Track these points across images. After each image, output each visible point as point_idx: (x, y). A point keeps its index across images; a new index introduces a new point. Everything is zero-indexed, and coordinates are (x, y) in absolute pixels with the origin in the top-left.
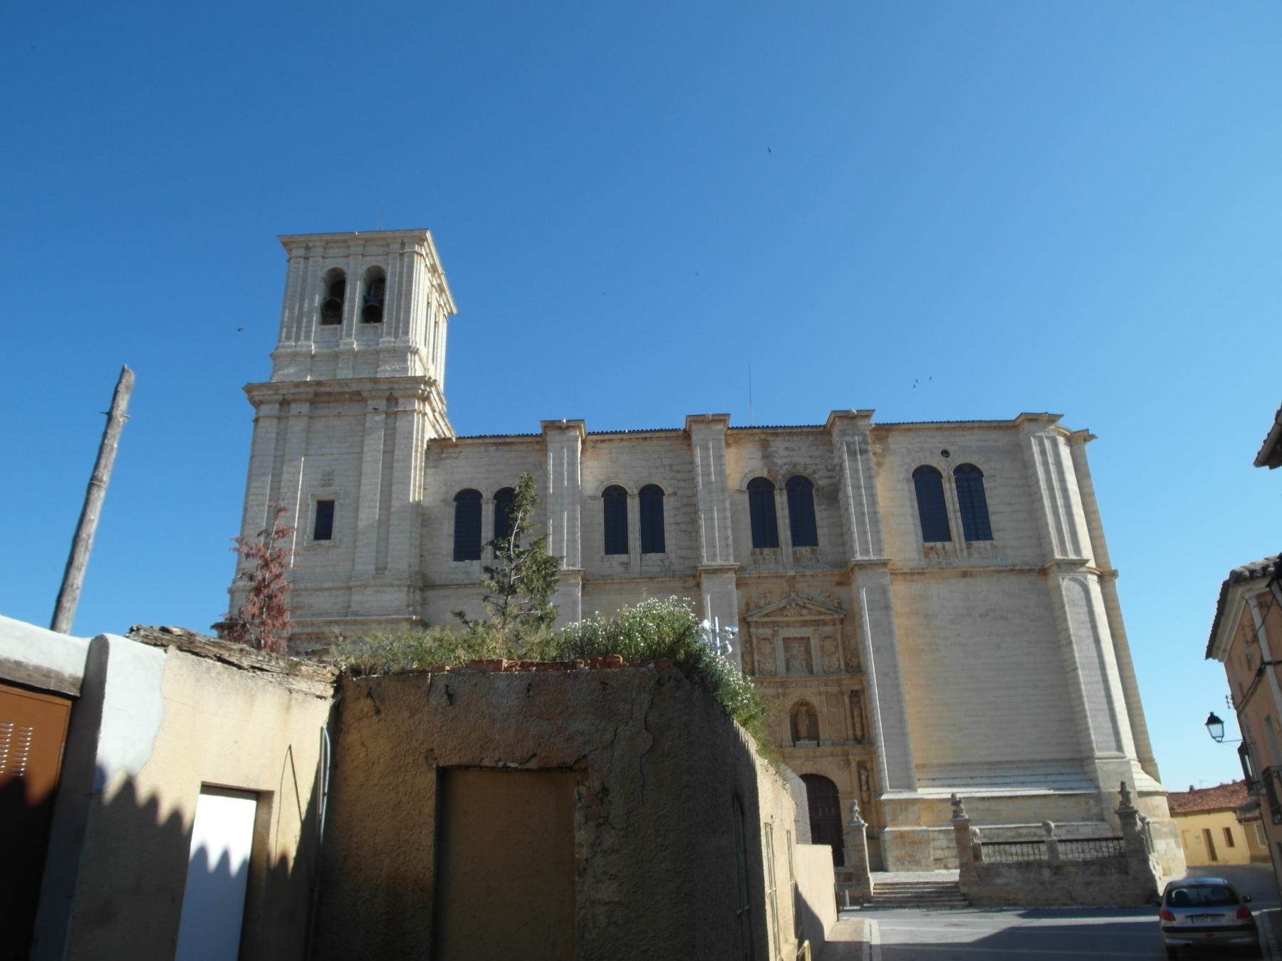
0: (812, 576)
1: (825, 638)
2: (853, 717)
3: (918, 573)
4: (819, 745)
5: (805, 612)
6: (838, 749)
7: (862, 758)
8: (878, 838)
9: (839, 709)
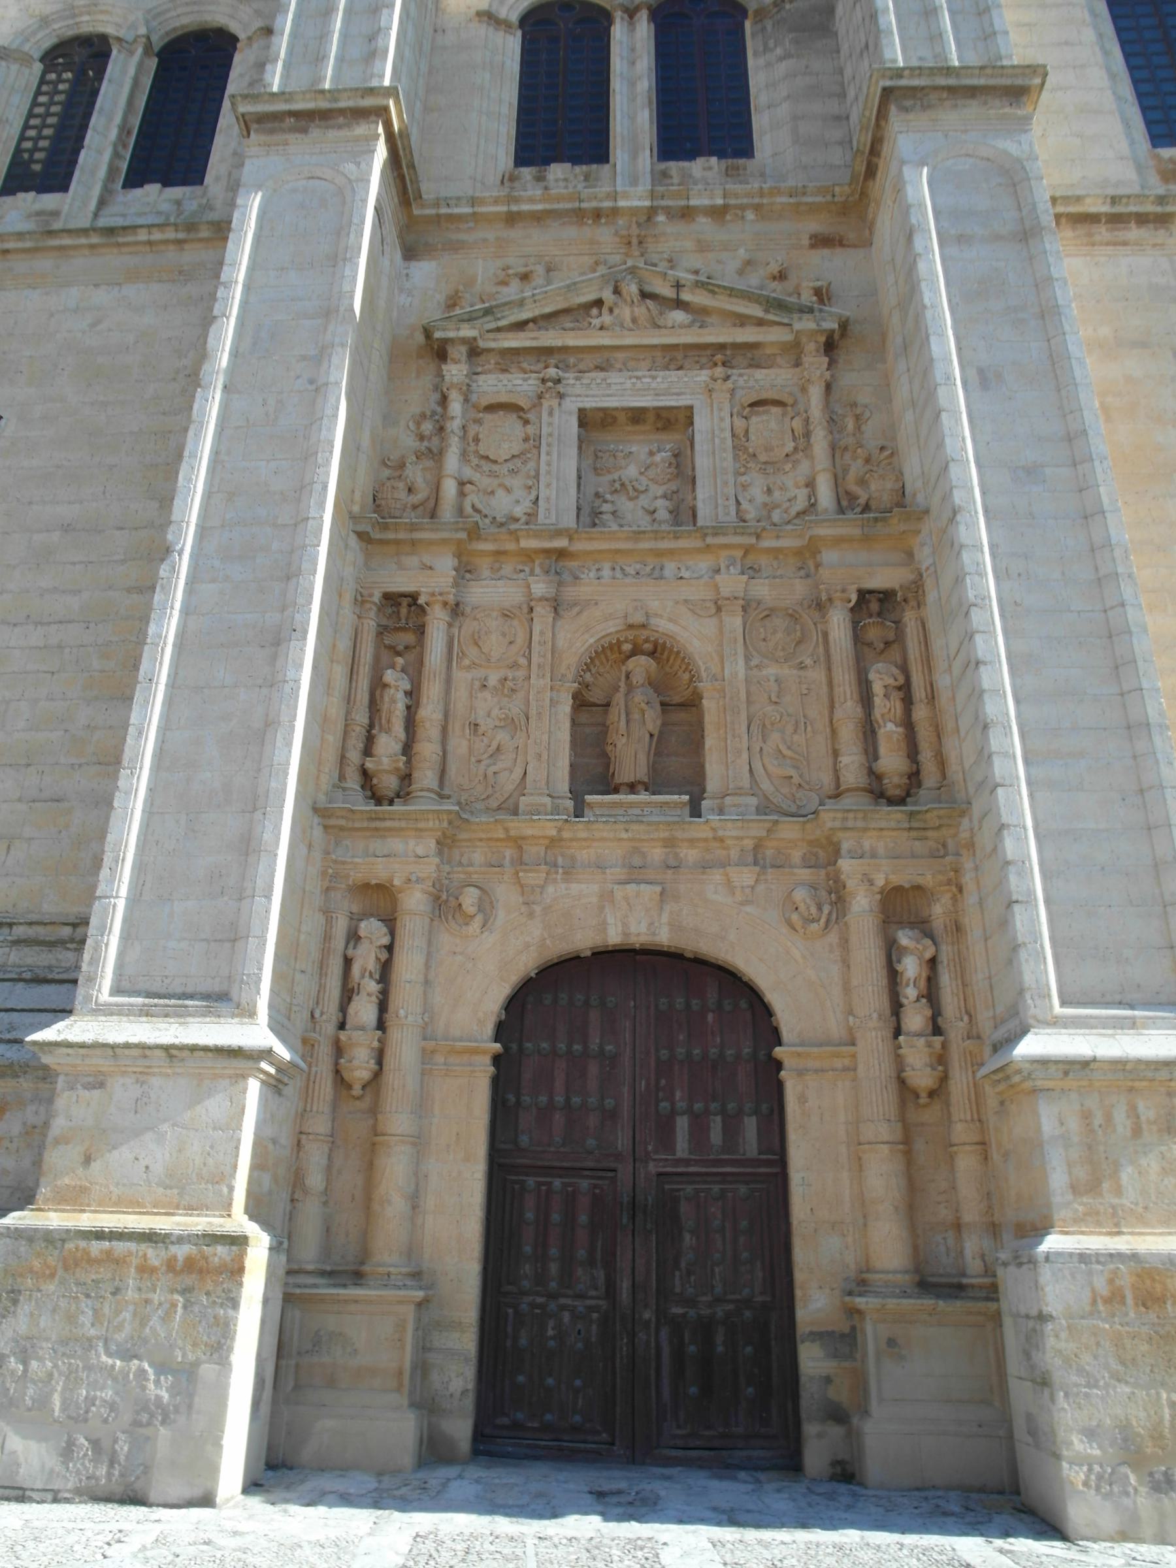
0: (718, 213)
1: (752, 405)
2: (866, 699)
3: (1142, 219)
4: (696, 812)
5: (679, 316)
6: (789, 830)
7: (903, 878)
8: (992, 1292)
9: (802, 667)
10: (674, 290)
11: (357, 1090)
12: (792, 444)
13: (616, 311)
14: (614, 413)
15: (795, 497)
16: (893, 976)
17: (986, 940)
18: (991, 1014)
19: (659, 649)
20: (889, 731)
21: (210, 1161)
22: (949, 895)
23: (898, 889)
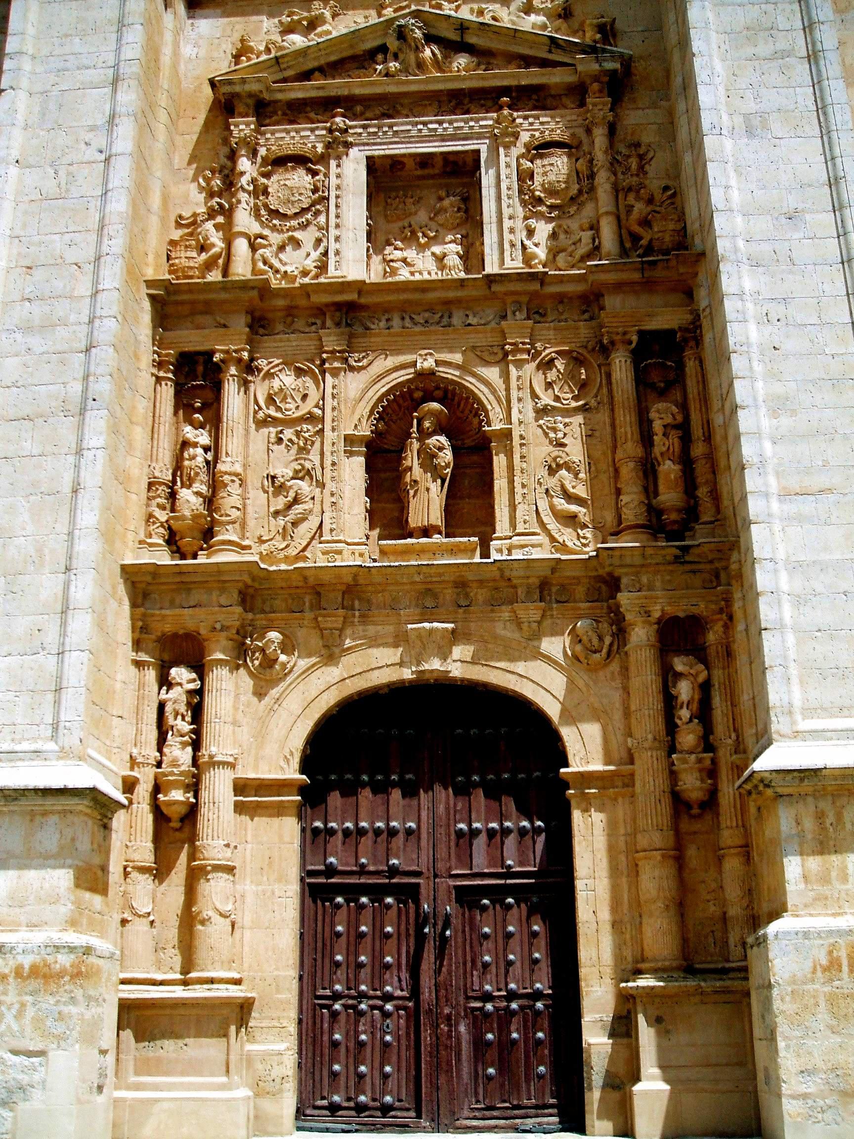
2: (646, 438)
8: (744, 971)
10: (459, 32)
11: (175, 824)
12: (577, 186)
13: (401, 56)
14: (402, 159)
15: (580, 240)
16: (669, 703)
17: (751, 663)
18: (754, 731)
19: (450, 396)
20: (669, 469)
21: (47, 885)
22: (721, 623)
23: (675, 619)
